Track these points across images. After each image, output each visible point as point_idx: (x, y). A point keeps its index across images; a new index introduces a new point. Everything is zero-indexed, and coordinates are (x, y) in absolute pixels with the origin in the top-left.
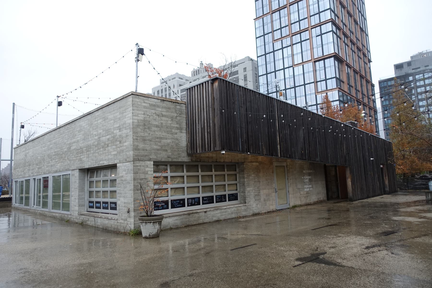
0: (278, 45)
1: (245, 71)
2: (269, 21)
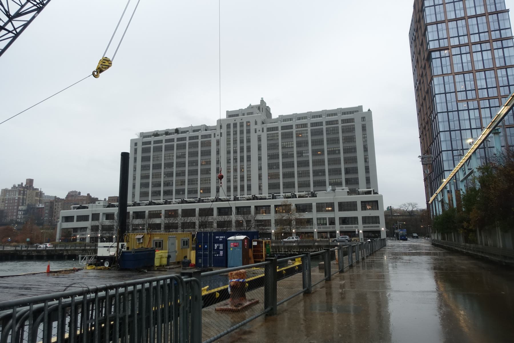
0: (463, 106)
1: (363, 120)
2: (452, 80)
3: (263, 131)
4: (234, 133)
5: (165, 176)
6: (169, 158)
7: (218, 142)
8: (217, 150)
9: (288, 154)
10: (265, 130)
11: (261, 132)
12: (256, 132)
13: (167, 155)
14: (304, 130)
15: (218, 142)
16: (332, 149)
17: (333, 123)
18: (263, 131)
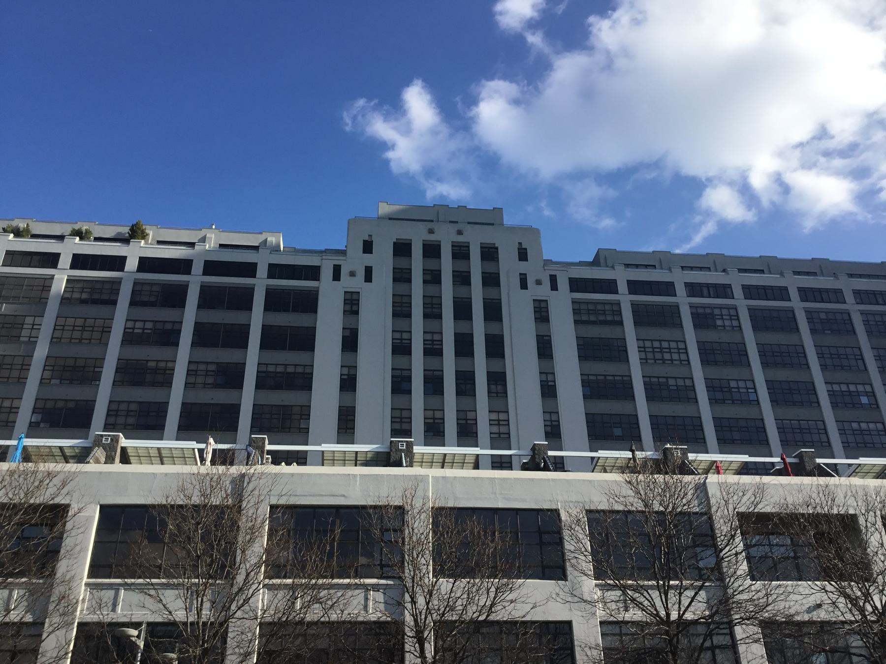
3: (554, 287)
4: (429, 277)
5: (36, 418)
6: (81, 339)
7: (352, 304)
8: (347, 333)
9: (667, 384)
10: (563, 284)
11: (544, 291)
12: (524, 285)
13: (70, 321)
14: (721, 307)
15: (352, 304)
16: (844, 388)
17: (825, 296)
18: (554, 287)
